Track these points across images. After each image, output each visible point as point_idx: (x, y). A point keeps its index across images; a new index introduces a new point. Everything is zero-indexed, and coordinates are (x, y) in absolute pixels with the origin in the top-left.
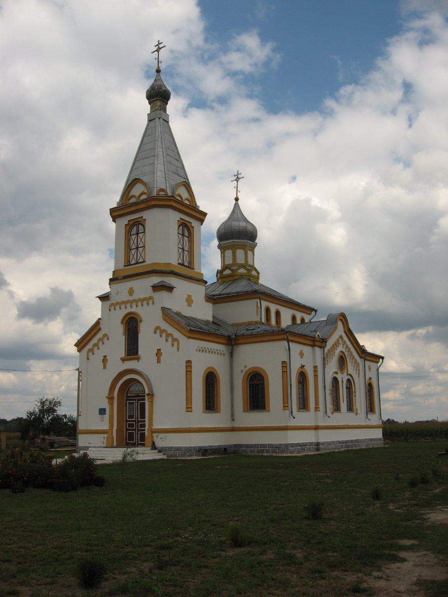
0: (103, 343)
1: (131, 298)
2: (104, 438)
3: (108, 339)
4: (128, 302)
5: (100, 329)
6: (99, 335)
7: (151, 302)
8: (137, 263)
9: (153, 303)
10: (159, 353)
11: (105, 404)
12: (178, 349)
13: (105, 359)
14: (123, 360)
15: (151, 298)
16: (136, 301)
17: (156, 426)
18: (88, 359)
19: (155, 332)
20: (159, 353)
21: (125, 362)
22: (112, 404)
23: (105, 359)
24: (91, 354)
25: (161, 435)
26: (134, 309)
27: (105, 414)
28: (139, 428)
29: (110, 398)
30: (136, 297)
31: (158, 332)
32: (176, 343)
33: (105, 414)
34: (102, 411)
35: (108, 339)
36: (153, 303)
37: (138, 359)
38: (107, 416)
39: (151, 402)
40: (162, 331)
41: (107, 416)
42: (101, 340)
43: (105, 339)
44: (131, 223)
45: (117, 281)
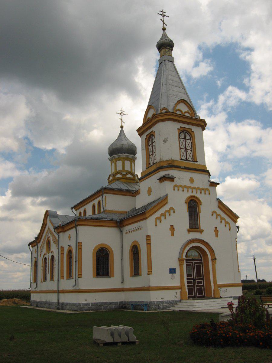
0: (170, 215)
1: (192, 186)
2: (176, 293)
3: (174, 212)
4: (190, 187)
5: (167, 203)
6: (166, 208)
7: (207, 192)
8: (187, 160)
9: (209, 194)
10: (216, 230)
11: (176, 265)
12: (230, 230)
13: (172, 228)
14: (189, 231)
15: (208, 190)
16: (197, 189)
17: (219, 282)
18: (156, 225)
19: (212, 215)
20: (216, 230)
21: (190, 233)
22: (181, 265)
23: (172, 228)
24: (158, 221)
25: (223, 289)
26: (194, 194)
27: (175, 273)
28: (197, 285)
29: (181, 260)
30: (195, 185)
31: (215, 215)
32: (227, 225)
33: (175, 273)
34: (172, 271)
35: (174, 212)
36: (209, 194)
37: (201, 232)
38: (177, 275)
39: (214, 265)
40: (218, 215)
41: (177, 275)
42: (168, 211)
43: (172, 212)
44: (182, 129)
45: (179, 169)
